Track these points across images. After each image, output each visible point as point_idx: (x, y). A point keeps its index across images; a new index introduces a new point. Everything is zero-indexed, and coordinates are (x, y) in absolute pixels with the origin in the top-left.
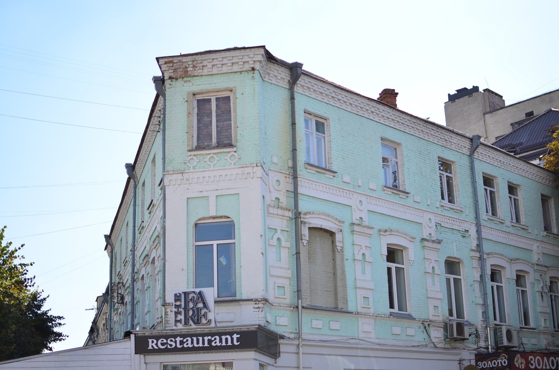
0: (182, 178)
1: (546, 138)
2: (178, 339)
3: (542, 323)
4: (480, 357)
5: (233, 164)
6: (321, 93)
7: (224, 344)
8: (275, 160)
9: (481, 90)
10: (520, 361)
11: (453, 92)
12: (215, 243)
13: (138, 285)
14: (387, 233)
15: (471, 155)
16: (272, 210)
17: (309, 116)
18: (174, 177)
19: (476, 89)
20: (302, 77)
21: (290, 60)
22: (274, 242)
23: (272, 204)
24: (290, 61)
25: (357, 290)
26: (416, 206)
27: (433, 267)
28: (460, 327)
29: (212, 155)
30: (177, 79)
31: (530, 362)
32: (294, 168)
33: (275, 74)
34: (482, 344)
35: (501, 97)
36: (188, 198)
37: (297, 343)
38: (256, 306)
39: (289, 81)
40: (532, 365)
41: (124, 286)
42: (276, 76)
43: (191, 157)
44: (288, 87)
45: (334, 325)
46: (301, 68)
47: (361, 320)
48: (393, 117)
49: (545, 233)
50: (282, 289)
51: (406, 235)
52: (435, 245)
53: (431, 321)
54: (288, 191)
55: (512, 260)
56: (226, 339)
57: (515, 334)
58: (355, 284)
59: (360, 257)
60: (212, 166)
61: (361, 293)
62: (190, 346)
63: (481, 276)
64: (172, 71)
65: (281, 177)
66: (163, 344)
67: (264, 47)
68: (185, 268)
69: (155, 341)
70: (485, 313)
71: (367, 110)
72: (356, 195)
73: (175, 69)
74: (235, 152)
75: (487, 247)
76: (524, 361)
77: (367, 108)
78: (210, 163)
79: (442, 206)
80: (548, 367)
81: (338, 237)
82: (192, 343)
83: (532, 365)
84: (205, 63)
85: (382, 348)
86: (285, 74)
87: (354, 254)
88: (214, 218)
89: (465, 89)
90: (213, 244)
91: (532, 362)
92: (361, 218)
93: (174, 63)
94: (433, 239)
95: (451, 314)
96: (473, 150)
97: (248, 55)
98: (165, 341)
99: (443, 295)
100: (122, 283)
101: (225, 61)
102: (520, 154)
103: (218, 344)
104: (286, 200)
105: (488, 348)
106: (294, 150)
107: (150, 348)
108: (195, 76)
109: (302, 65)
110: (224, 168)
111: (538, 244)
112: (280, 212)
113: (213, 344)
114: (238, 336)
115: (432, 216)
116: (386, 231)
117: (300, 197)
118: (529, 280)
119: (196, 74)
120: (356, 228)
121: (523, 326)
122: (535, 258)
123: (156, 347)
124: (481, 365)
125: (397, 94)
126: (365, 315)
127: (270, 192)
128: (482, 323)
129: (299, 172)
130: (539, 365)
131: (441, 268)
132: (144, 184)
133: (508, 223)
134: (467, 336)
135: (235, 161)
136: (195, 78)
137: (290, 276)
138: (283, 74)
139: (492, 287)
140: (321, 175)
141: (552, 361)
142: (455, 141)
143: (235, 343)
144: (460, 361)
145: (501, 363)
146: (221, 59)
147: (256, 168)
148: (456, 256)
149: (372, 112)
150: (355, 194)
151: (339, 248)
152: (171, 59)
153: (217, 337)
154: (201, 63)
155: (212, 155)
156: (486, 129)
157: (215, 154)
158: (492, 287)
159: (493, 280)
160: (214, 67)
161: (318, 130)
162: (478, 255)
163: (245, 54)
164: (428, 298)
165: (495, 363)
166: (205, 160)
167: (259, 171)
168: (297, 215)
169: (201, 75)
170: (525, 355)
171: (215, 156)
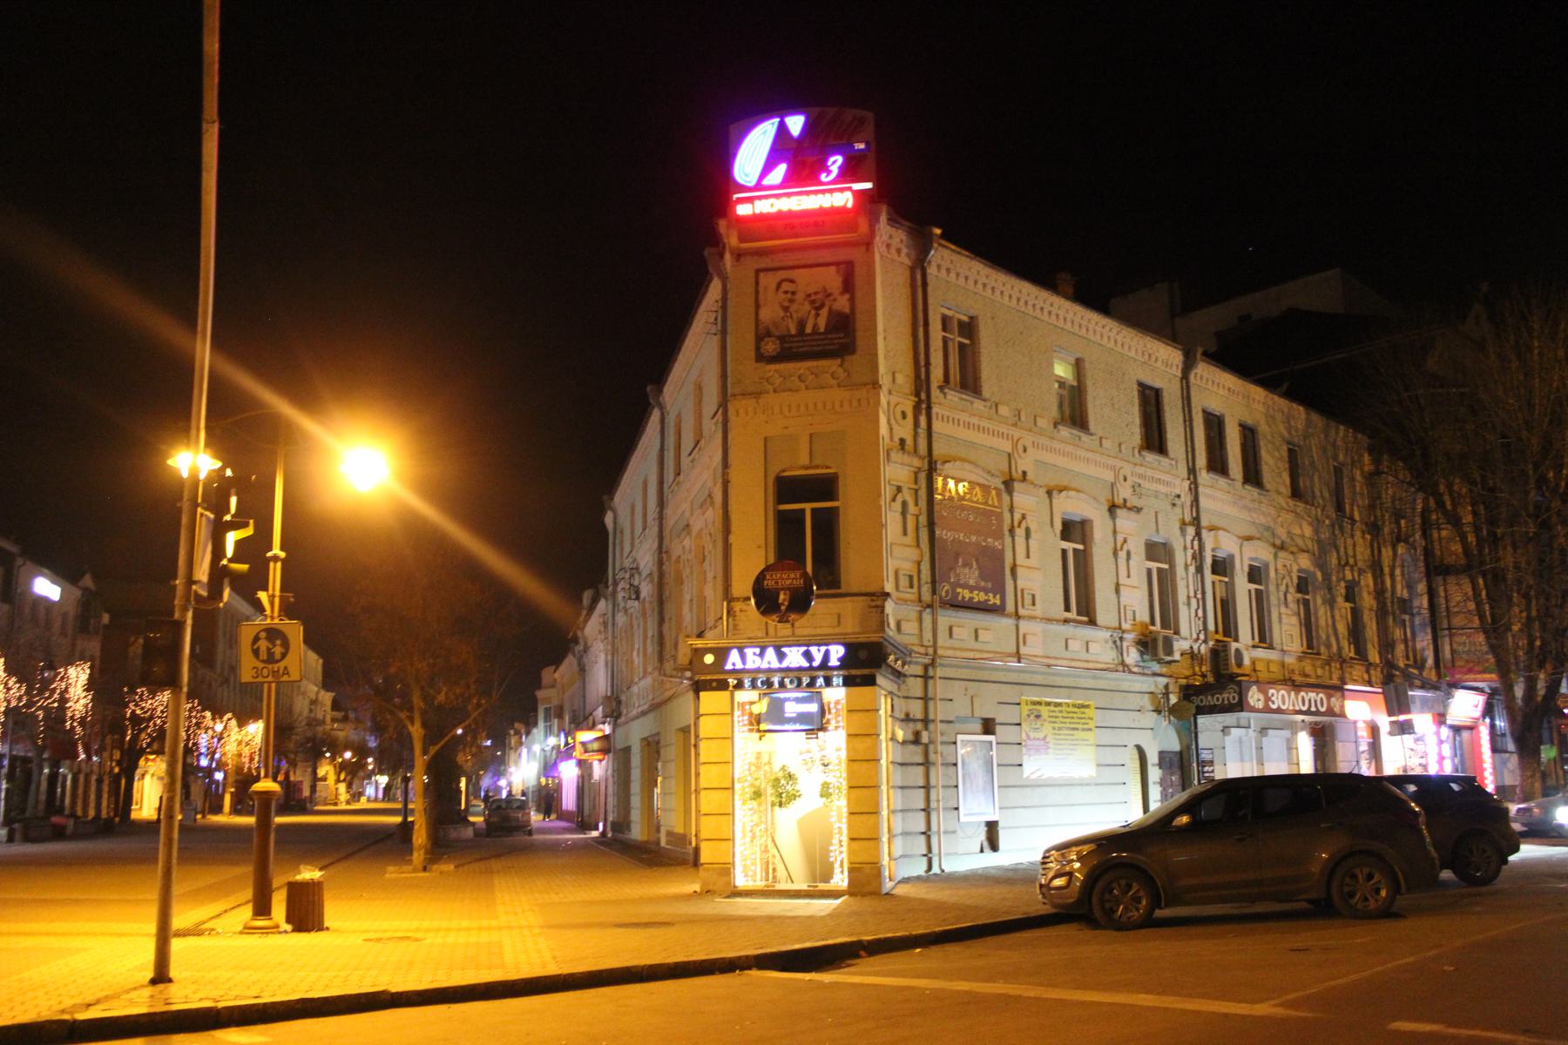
12: (808, 507)
40: (1273, 703)
76: (1262, 697)
83: (1273, 703)
90: (803, 511)
91: (1273, 698)
130: (1284, 704)
139: (1213, 583)
165: (1218, 699)
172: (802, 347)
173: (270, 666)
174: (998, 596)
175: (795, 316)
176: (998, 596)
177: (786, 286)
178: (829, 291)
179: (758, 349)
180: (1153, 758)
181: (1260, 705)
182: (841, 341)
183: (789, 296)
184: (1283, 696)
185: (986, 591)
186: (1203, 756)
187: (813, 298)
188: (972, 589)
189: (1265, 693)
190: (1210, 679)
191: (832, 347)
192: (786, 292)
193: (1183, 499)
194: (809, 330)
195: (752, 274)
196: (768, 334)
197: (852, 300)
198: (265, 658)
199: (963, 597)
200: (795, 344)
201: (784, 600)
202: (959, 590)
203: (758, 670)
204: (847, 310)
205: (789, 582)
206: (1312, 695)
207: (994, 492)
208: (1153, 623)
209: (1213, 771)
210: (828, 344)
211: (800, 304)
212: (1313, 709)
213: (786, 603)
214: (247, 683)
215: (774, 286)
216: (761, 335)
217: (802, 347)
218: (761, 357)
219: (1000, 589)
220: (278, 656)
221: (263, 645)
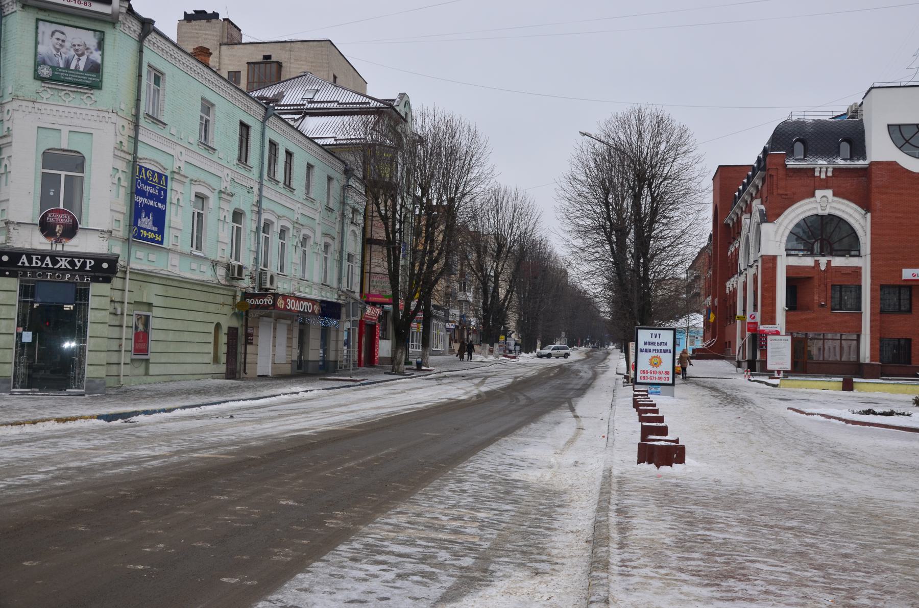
0: (33, 106)
3: (293, 271)
5: (88, 105)
6: (163, 50)
8: (123, 107)
11: (190, 11)
12: (63, 174)
15: (263, 122)
17: (150, 69)
18: (24, 103)
19: (215, 15)
20: (153, 34)
21: (145, 14)
23: (118, 146)
27: (225, 216)
29: (67, 92)
31: (287, 304)
32: (137, 116)
33: (130, 25)
35: (240, 30)
38: (102, 236)
39: (140, 34)
40: (288, 306)
42: (129, 27)
43: (45, 89)
45: (152, 257)
46: (153, 25)
47: (171, 255)
48: (213, 80)
50: (118, 222)
51: (210, 186)
52: (228, 198)
53: (218, 261)
55: (279, 217)
57: (276, 279)
60: (67, 102)
63: (257, 228)
65: (125, 123)
68: (32, 193)
70: (256, 259)
71: (195, 71)
75: (265, 204)
77: (195, 69)
80: (298, 309)
86: (136, 27)
88: (64, 150)
89: (204, 12)
92: (179, 167)
94: (227, 192)
96: (266, 118)
99: (228, 241)
104: (128, 146)
106: (138, 100)
109: (154, 22)
110: (79, 107)
111: (299, 205)
112: (123, 155)
116: (196, 181)
117: (139, 144)
122: (295, 217)
124: (249, 301)
125: (211, 54)
126: (174, 252)
127: (116, 135)
128: (251, 266)
135: (91, 103)
137: (125, 212)
138: (136, 26)
140: (155, 125)
142: (254, 108)
147: (111, 115)
148: (242, 208)
149: (198, 73)
150: (177, 146)
155: (67, 92)
156: (219, 60)
157: (71, 91)
161: (155, 83)
162: (256, 209)
164: (218, 241)
165: (261, 302)
166: (60, 95)
170: (284, 297)
171: (70, 93)
172: (66, 76)
174: (160, 236)
175: (63, 56)
176: (160, 236)
177: (58, 35)
178: (87, 46)
179: (36, 70)
180: (225, 329)
181: (282, 307)
182: (94, 79)
183: (60, 42)
185: (155, 233)
186: (249, 331)
187: (77, 47)
188: (148, 231)
189: (285, 301)
191: (87, 81)
192: (58, 39)
193: (254, 190)
194: (72, 67)
195: (34, 21)
196: (44, 63)
197: (102, 55)
199: (143, 235)
200: (62, 74)
201: (59, 230)
202: (142, 231)
203: (40, 268)
204: (99, 61)
205: (63, 220)
206: (306, 303)
207: (164, 177)
208: (231, 257)
209: (252, 339)
210: (85, 79)
211: (67, 49)
212: (306, 311)
213: (60, 232)
215: (50, 33)
216: (39, 62)
217: (66, 76)
218: (38, 77)
219: (161, 232)
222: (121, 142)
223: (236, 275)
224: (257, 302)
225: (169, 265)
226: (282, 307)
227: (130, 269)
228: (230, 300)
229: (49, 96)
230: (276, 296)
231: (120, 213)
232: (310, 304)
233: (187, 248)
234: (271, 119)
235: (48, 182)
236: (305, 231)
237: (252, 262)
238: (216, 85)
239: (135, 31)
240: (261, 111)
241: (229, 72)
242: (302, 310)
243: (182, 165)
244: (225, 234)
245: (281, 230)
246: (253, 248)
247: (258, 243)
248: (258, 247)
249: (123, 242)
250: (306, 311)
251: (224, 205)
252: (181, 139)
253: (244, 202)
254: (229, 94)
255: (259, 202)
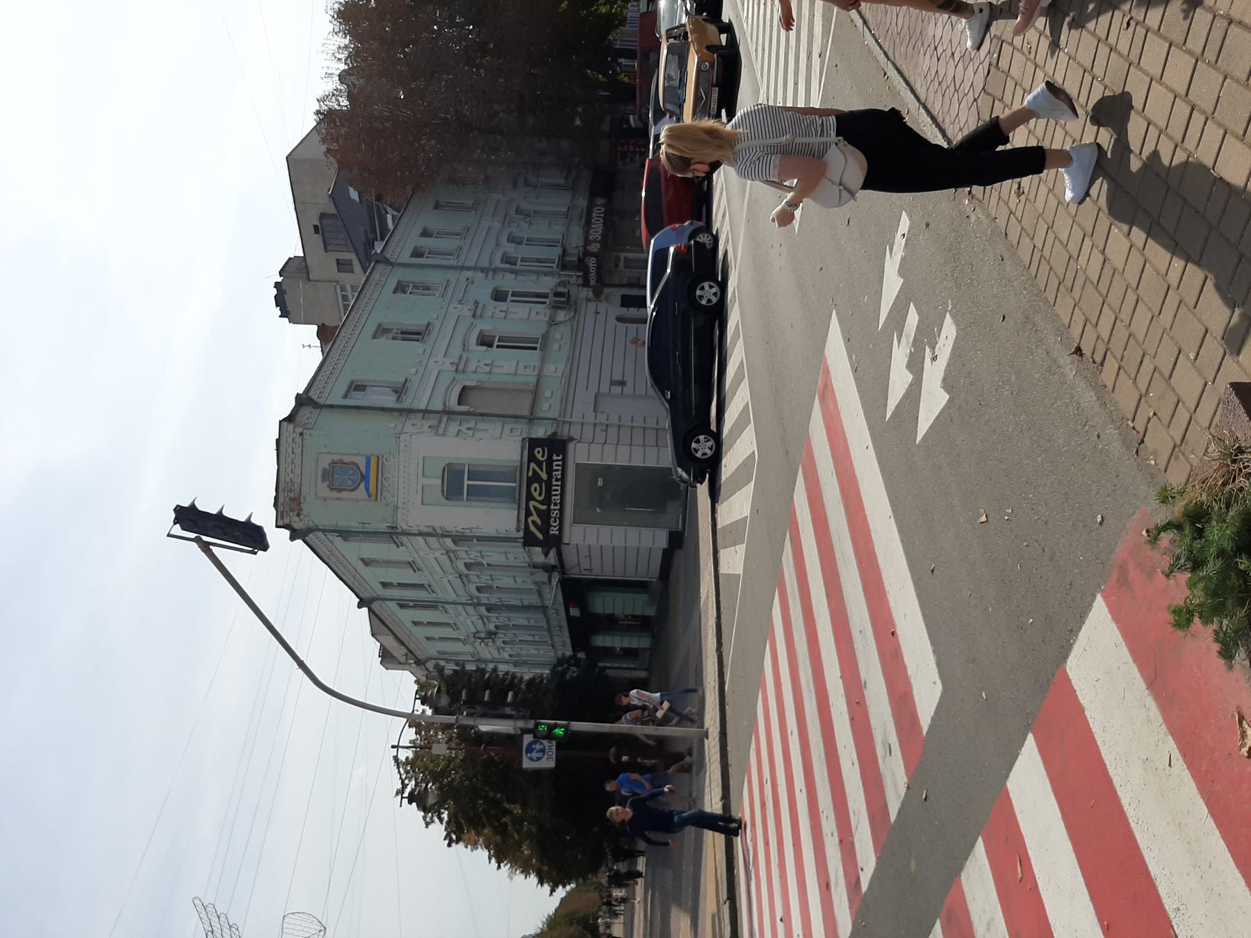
1: (363, 204)
2: (552, 507)
4: (586, 283)
7: (560, 468)
8: (393, 426)
9: (280, 279)
10: (594, 247)
12: (466, 482)
13: (484, 597)
14: (467, 344)
16: (441, 431)
17: (349, 396)
18: (400, 516)
19: (277, 285)
20: (311, 394)
22: (470, 433)
24: (293, 404)
25: (518, 373)
26: (441, 318)
28: (557, 294)
30: (301, 510)
33: (306, 418)
34: (573, 280)
35: (290, 259)
36: (422, 504)
37: (561, 422)
39: (313, 408)
40: (597, 238)
41: (478, 632)
42: (308, 418)
44: (319, 410)
45: (548, 394)
47: (545, 373)
49: (473, 211)
53: (550, 319)
54: (423, 418)
55: (498, 245)
56: (557, 465)
58: (512, 374)
59: (487, 369)
61: (521, 370)
62: (559, 497)
63: (512, 272)
64: (292, 513)
65: (409, 424)
66: (555, 522)
67: (280, 421)
68: (488, 510)
69: (552, 528)
70: (546, 274)
71: (344, 347)
72: (429, 365)
73: (290, 509)
74: (383, 457)
75: (484, 263)
76: (593, 244)
78: (391, 482)
79: (442, 297)
80: (601, 225)
81: (468, 383)
82: (557, 495)
84: (288, 480)
85: (572, 359)
86: (306, 412)
87: (485, 373)
89: (275, 297)
90: (468, 485)
91: (595, 237)
93: (283, 511)
94: (474, 307)
95: (544, 303)
96: (387, 262)
97: (287, 438)
98: (553, 519)
100: (475, 633)
101: (289, 460)
102: (376, 236)
103: (560, 473)
104: (432, 421)
105: (578, 276)
106: (383, 409)
107: (557, 532)
108: (300, 491)
109: (298, 394)
112: (443, 425)
113: (559, 477)
114: (555, 455)
115: (451, 308)
116: (464, 345)
117: (429, 408)
118: (517, 232)
119: (299, 490)
120: (461, 367)
121: (560, 245)
122: (496, 225)
123: (557, 528)
124: (593, 282)
129: (405, 407)
130: (598, 232)
131: (502, 306)
132: (384, 585)
133: (461, 243)
134: (565, 290)
136: (302, 491)
137: (501, 423)
141: (596, 220)
143: (560, 458)
144: (588, 300)
145: (594, 264)
146: (287, 465)
148: (491, 291)
151: (479, 384)
152: (279, 514)
153: (555, 473)
154: (288, 483)
157: (382, 475)
158: (522, 265)
159: (515, 264)
160: (294, 471)
161: (364, 390)
162: (490, 276)
163: (285, 441)
165: (593, 270)
167: (403, 437)
168: (448, 413)
169: (301, 484)
170: (587, 242)
171: (384, 476)
173: (547, 751)
180: (623, 311)
184: (594, 232)
190: (581, 274)
198: (542, 753)
206: (594, 215)
208: (544, 303)
212: (602, 215)
214: (556, 764)
220: (542, 747)
221: (534, 755)
222: (430, 427)
223: (564, 299)
224: (593, 275)
225: (553, 375)
226: (598, 245)
227: (560, 417)
228: (592, 306)
229: (389, 495)
230: (587, 253)
231: (503, 427)
232: (595, 209)
233: (537, 353)
234: (388, 256)
235: (475, 493)
236: (513, 212)
237: (549, 279)
238: (357, 322)
239: (310, 413)
240: (380, 267)
241: (339, 272)
242: (602, 221)
243: (448, 360)
244: (521, 311)
245: (512, 242)
246: (534, 277)
247: (529, 271)
248: (534, 272)
249: (533, 425)
250: (602, 215)
251: (488, 313)
252: (420, 362)
253: (483, 289)
254: (365, 306)
255: (482, 270)
